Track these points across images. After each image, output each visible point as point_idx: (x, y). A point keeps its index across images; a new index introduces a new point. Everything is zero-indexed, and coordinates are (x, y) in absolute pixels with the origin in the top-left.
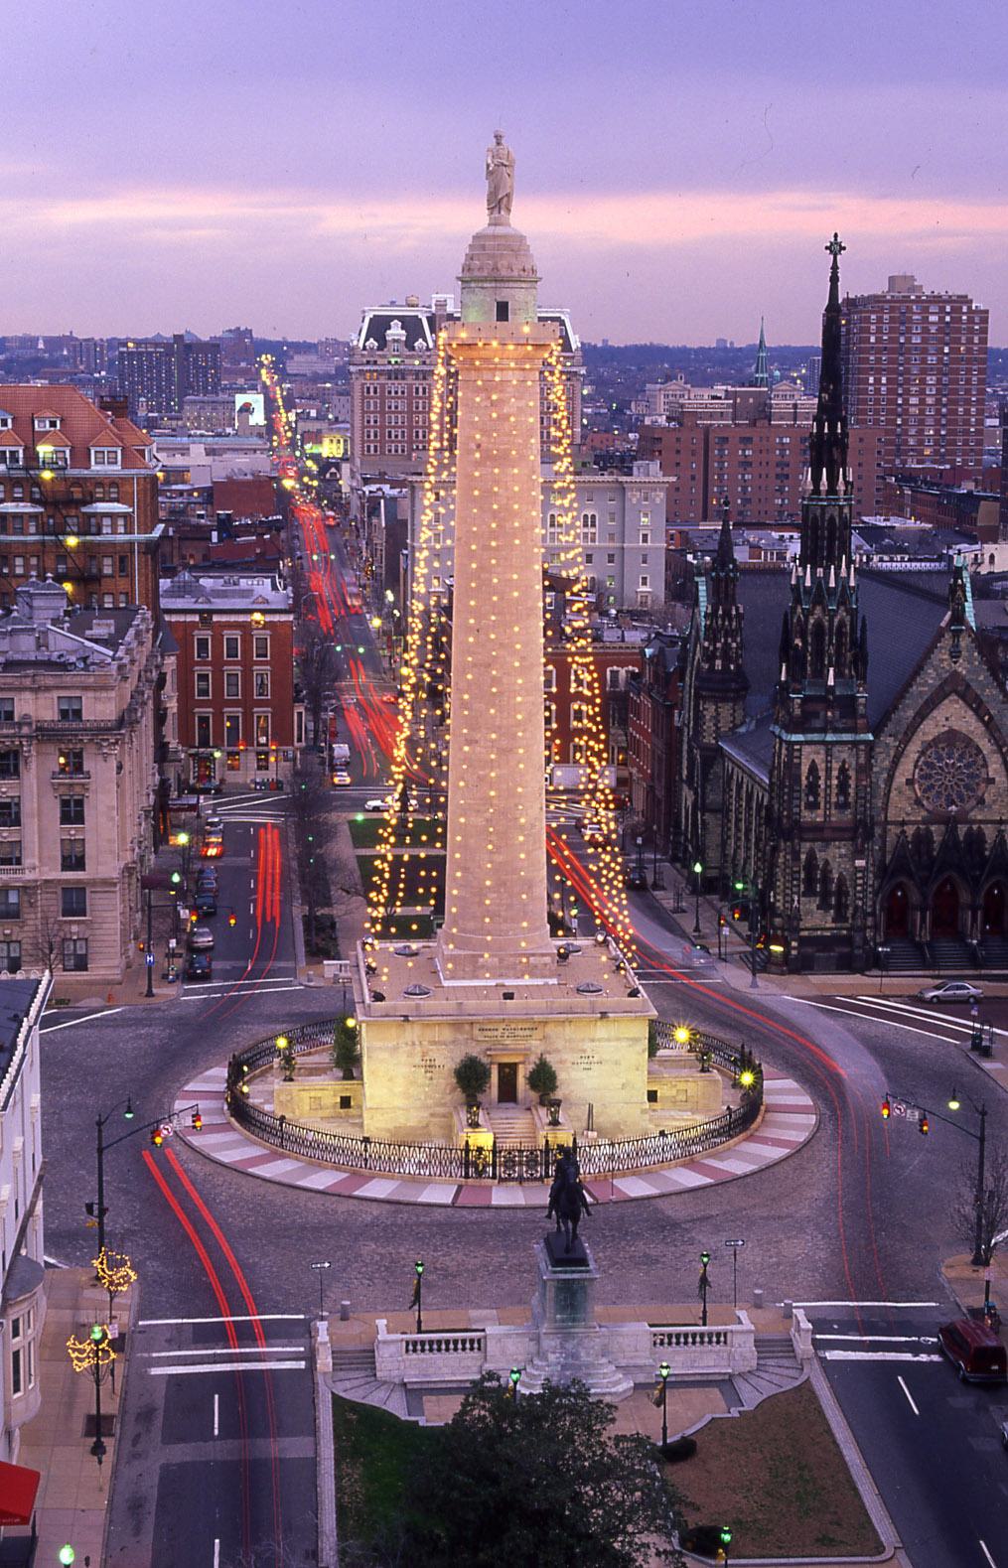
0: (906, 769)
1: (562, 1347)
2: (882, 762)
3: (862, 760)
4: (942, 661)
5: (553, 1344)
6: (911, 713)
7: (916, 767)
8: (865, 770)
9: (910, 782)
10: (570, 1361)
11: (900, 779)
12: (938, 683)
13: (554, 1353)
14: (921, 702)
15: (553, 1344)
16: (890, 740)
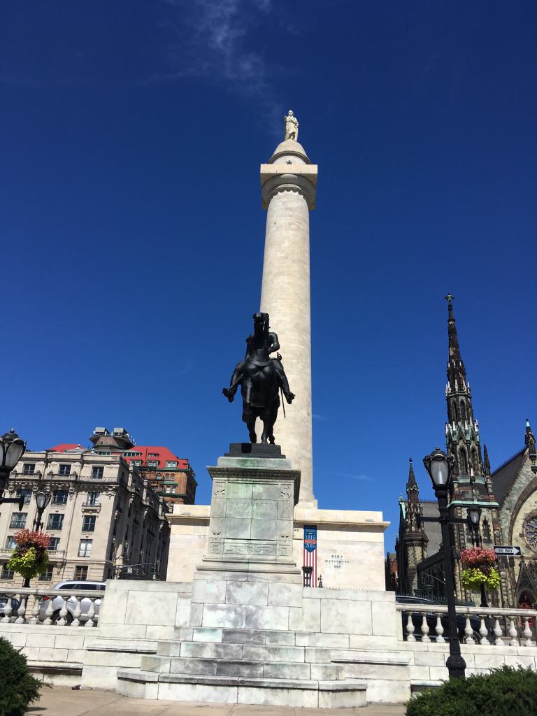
0: (518, 528)
1: (230, 597)
2: (505, 524)
3: (495, 517)
4: (528, 472)
5: (213, 588)
6: (515, 498)
7: (523, 527)
8: (497, 522)
9: (521, 535)
10: (243, 626)
11: (516, 534)
12: (528, 483)
13: (214, 608)
14: (520, 492)
15: (213, 588)
16: (507, 512)
